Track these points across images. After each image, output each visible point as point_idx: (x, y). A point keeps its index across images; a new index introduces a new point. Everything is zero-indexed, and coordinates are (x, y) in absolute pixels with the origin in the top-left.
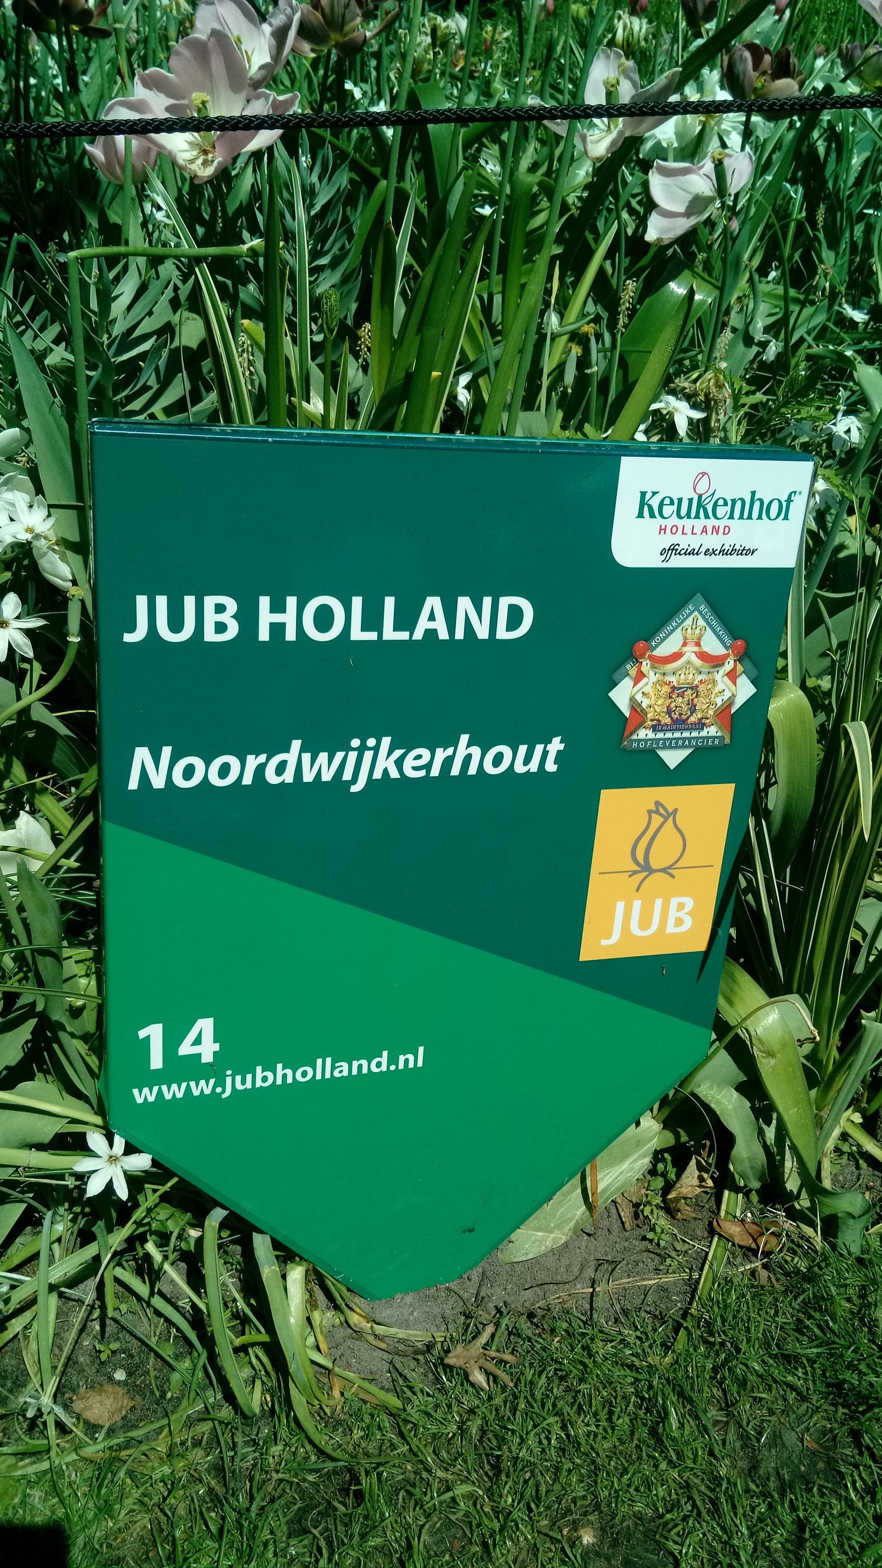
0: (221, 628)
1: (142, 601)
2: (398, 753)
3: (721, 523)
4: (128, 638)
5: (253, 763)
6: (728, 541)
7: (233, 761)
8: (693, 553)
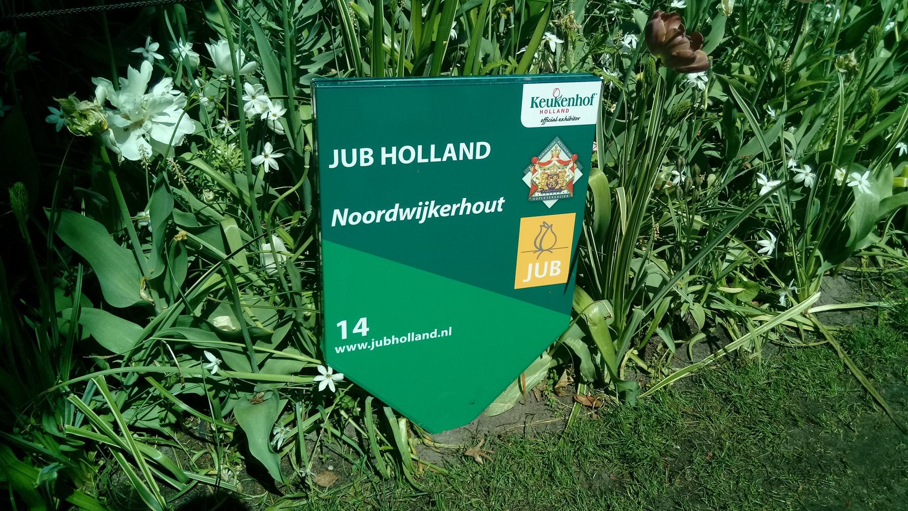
0: (367, 160)
1: (336, 152)
2: (438, 207)
3: (565, 108)
4: (331, 166)
5: (380, 213)
6: (568, 115)
7: (372, 213)
8: (554, 120)
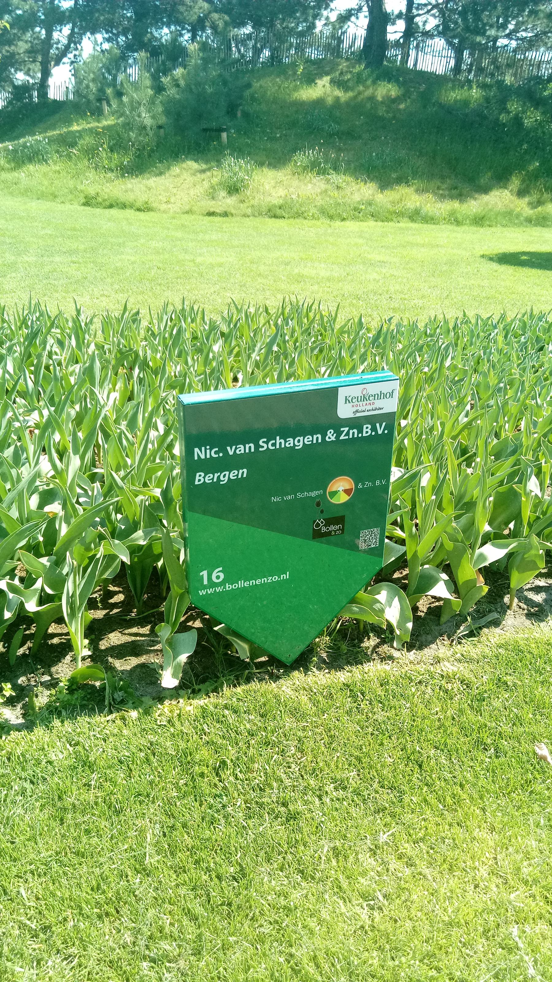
6: (374, 407)
